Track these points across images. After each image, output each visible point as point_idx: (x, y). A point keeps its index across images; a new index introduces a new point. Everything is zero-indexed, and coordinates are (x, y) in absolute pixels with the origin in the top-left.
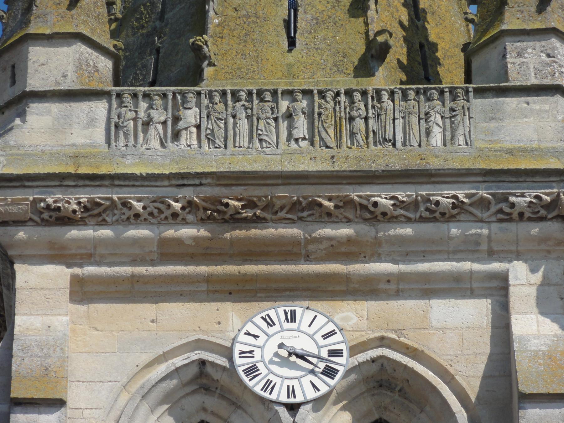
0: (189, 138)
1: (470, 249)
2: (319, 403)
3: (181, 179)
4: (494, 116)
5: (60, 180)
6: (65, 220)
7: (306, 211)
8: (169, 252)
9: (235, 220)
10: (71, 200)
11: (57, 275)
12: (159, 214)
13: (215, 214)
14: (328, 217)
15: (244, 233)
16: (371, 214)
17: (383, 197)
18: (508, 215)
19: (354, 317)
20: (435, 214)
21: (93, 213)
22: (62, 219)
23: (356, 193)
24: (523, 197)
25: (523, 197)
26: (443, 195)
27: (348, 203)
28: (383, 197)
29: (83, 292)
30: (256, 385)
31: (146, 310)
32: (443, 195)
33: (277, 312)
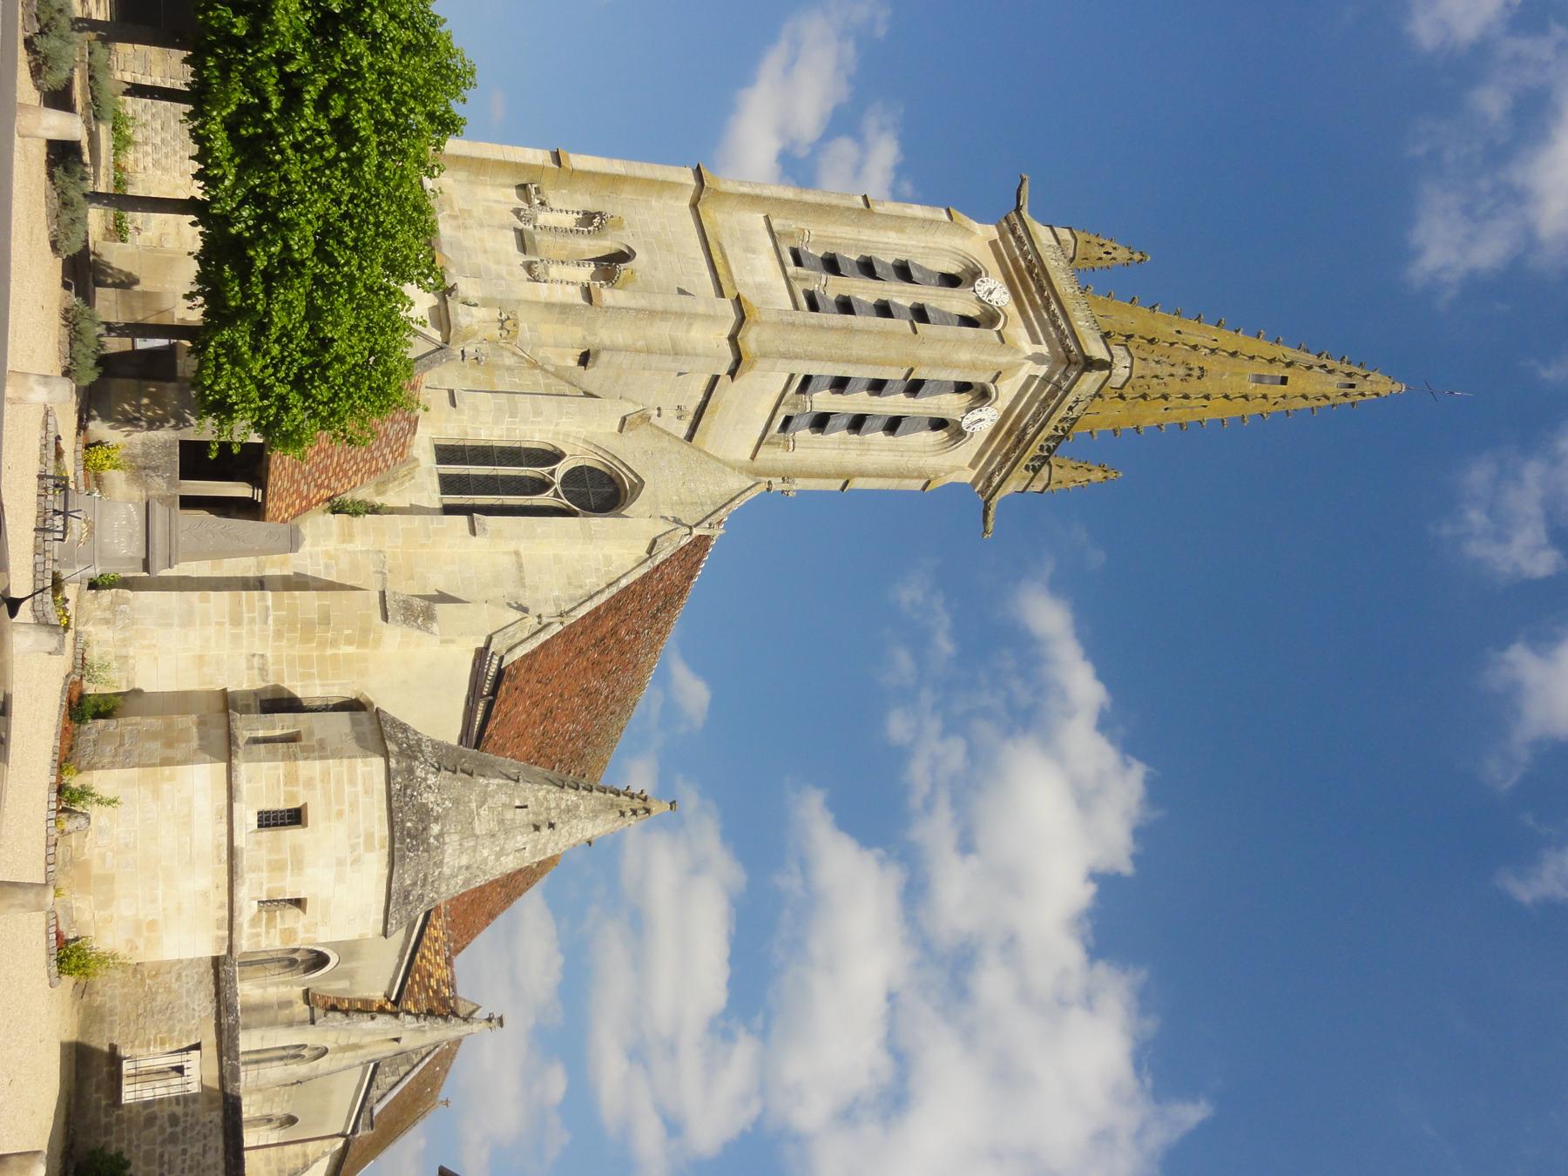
2: (979, 299)
3: (1038, 256)
6: (1013, 232)
7: (1041, 290)
8: (1015, 261)
9: (1031, 273)
10: (1020, 231)
11: (996, 235)
14: (1042, 296)
15: (1028, 278)
16: (1047, 307)
17: (1054, 306)
18: (1062, 342)
19: (1012, 309)
21: (1019, 239)
22: (1013, 232)
24: (1069, 342)
25: (1069, 342)
26: (1061, 322)
27: (1048, 299)
28: (1054, 306)
29: (993, 244)
32: (1061, 322)
33: (1005, 289)
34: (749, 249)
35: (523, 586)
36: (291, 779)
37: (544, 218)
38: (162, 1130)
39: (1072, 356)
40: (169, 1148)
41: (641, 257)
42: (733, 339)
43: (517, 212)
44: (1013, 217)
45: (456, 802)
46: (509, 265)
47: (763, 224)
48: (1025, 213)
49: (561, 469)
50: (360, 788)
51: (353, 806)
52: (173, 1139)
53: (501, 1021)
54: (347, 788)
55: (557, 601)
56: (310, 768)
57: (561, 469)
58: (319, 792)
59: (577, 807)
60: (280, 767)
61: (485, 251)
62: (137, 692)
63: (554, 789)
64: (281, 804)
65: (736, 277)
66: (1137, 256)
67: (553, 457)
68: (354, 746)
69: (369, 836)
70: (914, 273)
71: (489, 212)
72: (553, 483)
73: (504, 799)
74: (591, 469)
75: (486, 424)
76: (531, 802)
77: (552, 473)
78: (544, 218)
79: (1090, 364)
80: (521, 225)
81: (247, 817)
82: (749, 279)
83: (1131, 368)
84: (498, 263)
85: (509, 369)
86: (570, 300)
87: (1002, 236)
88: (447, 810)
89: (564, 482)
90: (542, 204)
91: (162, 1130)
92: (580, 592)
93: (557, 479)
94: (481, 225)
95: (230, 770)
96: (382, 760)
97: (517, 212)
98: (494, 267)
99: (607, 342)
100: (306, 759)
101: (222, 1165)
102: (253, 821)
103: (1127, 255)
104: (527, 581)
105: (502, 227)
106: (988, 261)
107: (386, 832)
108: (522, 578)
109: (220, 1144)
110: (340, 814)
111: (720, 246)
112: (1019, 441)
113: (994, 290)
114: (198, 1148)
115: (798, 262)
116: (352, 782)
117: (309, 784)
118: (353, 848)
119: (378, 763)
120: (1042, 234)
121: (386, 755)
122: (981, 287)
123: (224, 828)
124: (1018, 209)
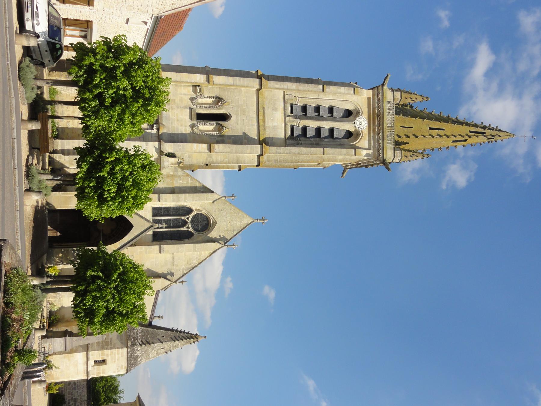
0: (388, 111)
1: (374, 145)
2: (355, 126)
3: (383, 110)
4: (391, 149)
5: (383, 95)
6: (378, 96)
7: (379, 125)
8: (374, 109)
10: (380, 97)
11: (371, 95)
12: (379, 107)
13: (378, 114)
14: (378, 128)
15: (376, 118)
16: (378, 134)
19: (366, 131)
20: (378, 141)
21: (379, 99)
22: (378, 96)
23: (381, 131)
24: (381, 152)
25: (381, 152)
26: (381, 142)
28: (380, 135)
29: (369, 98)
30: (357, 119)
31: (367, 106)
32: (381, 142)
33: (366, 122)
34: (275, 109)
35: (174, 265)
36: (103, 354)
37: (201, 100)
38: (72, 386)
39: (380, 158)
40: (74, 391)
41: (233, 118)
42: (259, 156)
43: (192, 99)
44: (380, 88)
45: (145, 352)
46: (185, 126)
47: (282, 96)
48: (385, 87)
49: (191, 216)
50: (120, 355)
51: (118, 360)
52: (75, 388)
53: (162, 317)
54: (117, 356)
55: (183, 269)
56: (108, 352)
57: (191, 216)
58: (110, 357)
59: (178, 345)
60: (100, 352)
61: (178, 120)
62: (62, 307)
63: (172, 342)
64: (100, 359)
65: (266, 124)
66: (425, 99)
67: (188, 211)
68: (119, 343)
69: (122, 366)
70: (335, 114)
71: (181, 100)
72: (187, 223)
73: (158, 348)
74: (201, 214)
75: (169, 201)
76: (166, 346)
77: (188, 218)
78: (201, 100)
79: (384, 162)
80: (192, 106)
81: (91, 363)
82: (271, 124)
83: (401, 160)
84: (182, 126)
85: (180, 177)
86: (203, 151)
87: (373, 95)
88: (143, 354)
89: (192, 221)
90: (201, 95)
91: (72, 386)
92: (190, 266)
93: (189, 221)
94: (178, 107)
95: (87, 354)
96: (126, 349)
97: (192, 99)
98: (180, 128)
99: (215, 161)
100: (107, 349)
101: (86, 396)
102: (93, 363)
103: (421, 99)
104: (175, 263)
105: (185, 107)
106: (365, 110)
107: (126, 365)
108: (174, 262)
109: (86, 391)
110: (115, 362)
111: (264, 108)
112: (358, 164)
113: (361, 123)
114: (81, 391)
115: (292, 112)
116: (118, 354)
117: (107, 355)
118: (118, 369)
119: (125, 350)
120: (389, 95)
121: (127, 347)
122: (357, 121)
123: (86, 366)
124: (383, 85)
